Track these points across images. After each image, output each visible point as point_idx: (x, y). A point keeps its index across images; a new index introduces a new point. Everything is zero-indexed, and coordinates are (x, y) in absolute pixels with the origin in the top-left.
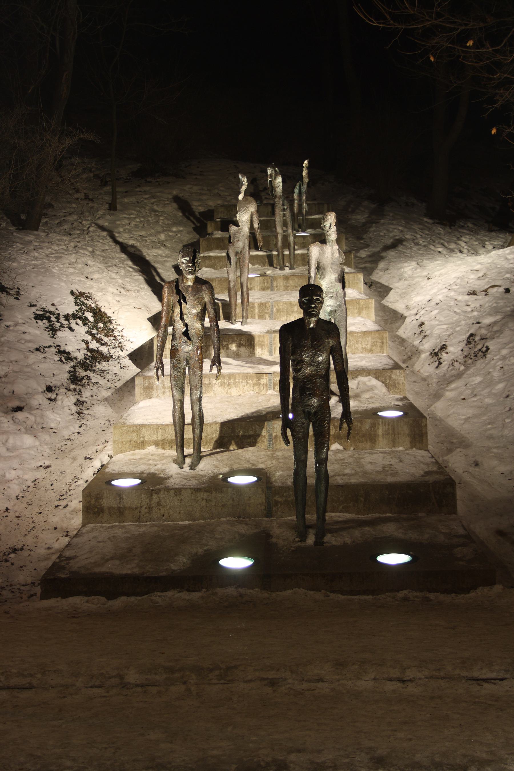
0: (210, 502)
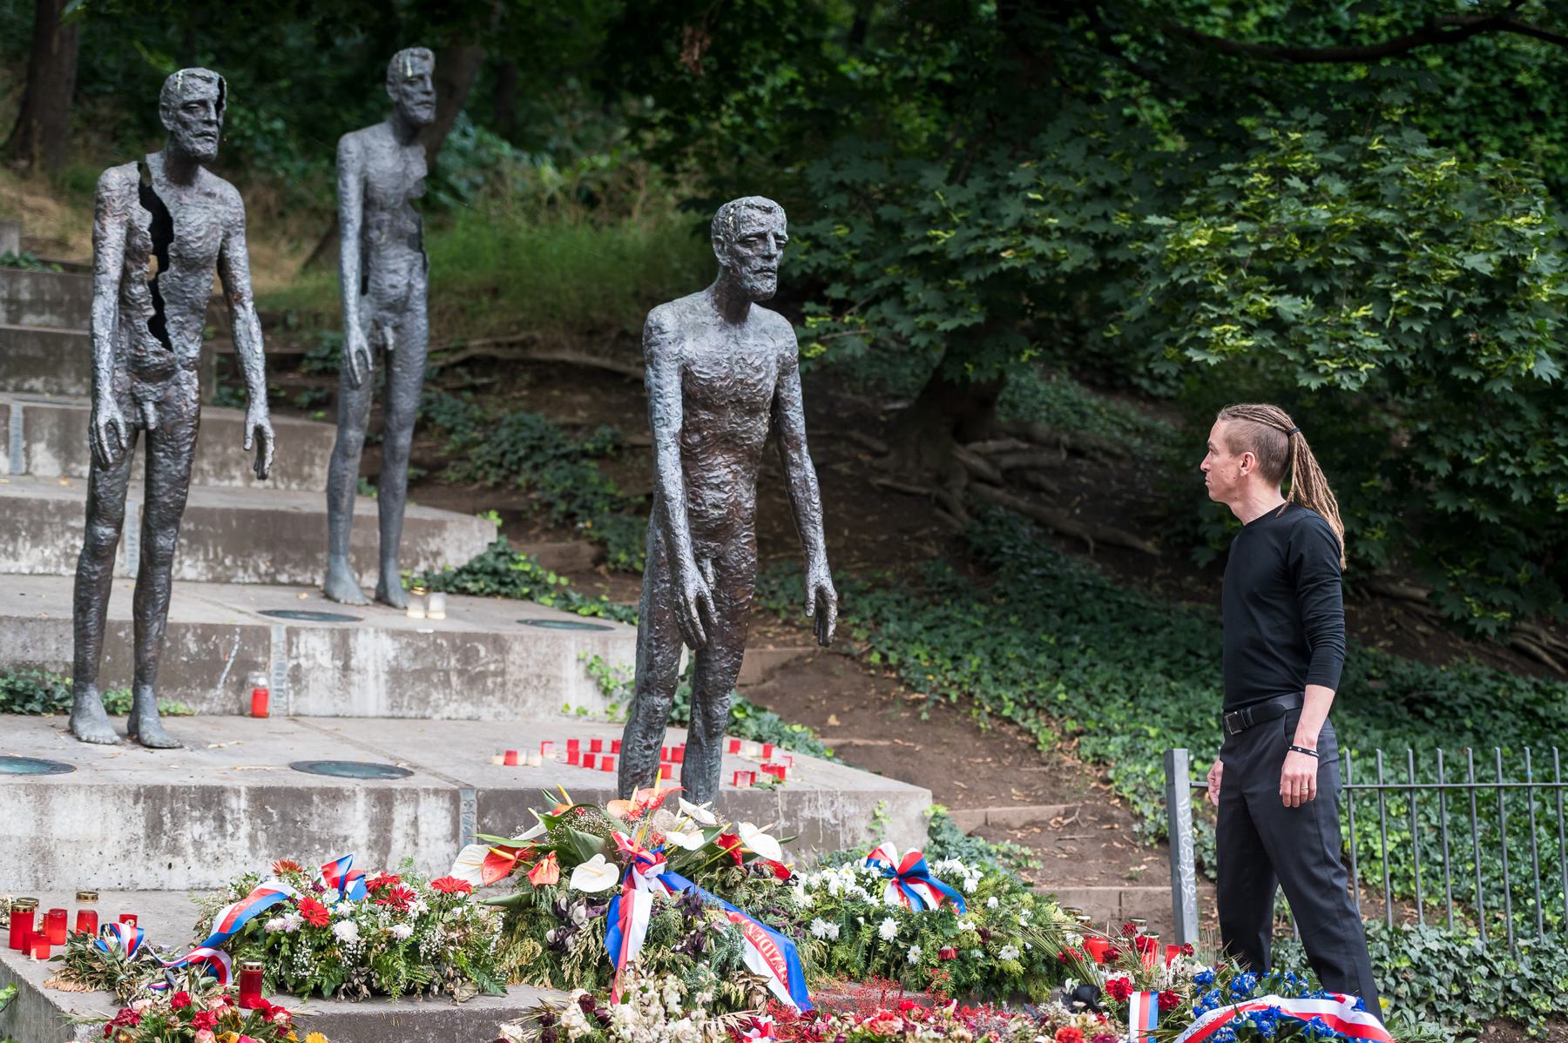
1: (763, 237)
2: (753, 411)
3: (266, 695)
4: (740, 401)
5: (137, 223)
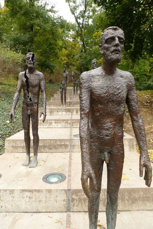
0: (32, 199)
2: (119, 103)
4: (113, 101)
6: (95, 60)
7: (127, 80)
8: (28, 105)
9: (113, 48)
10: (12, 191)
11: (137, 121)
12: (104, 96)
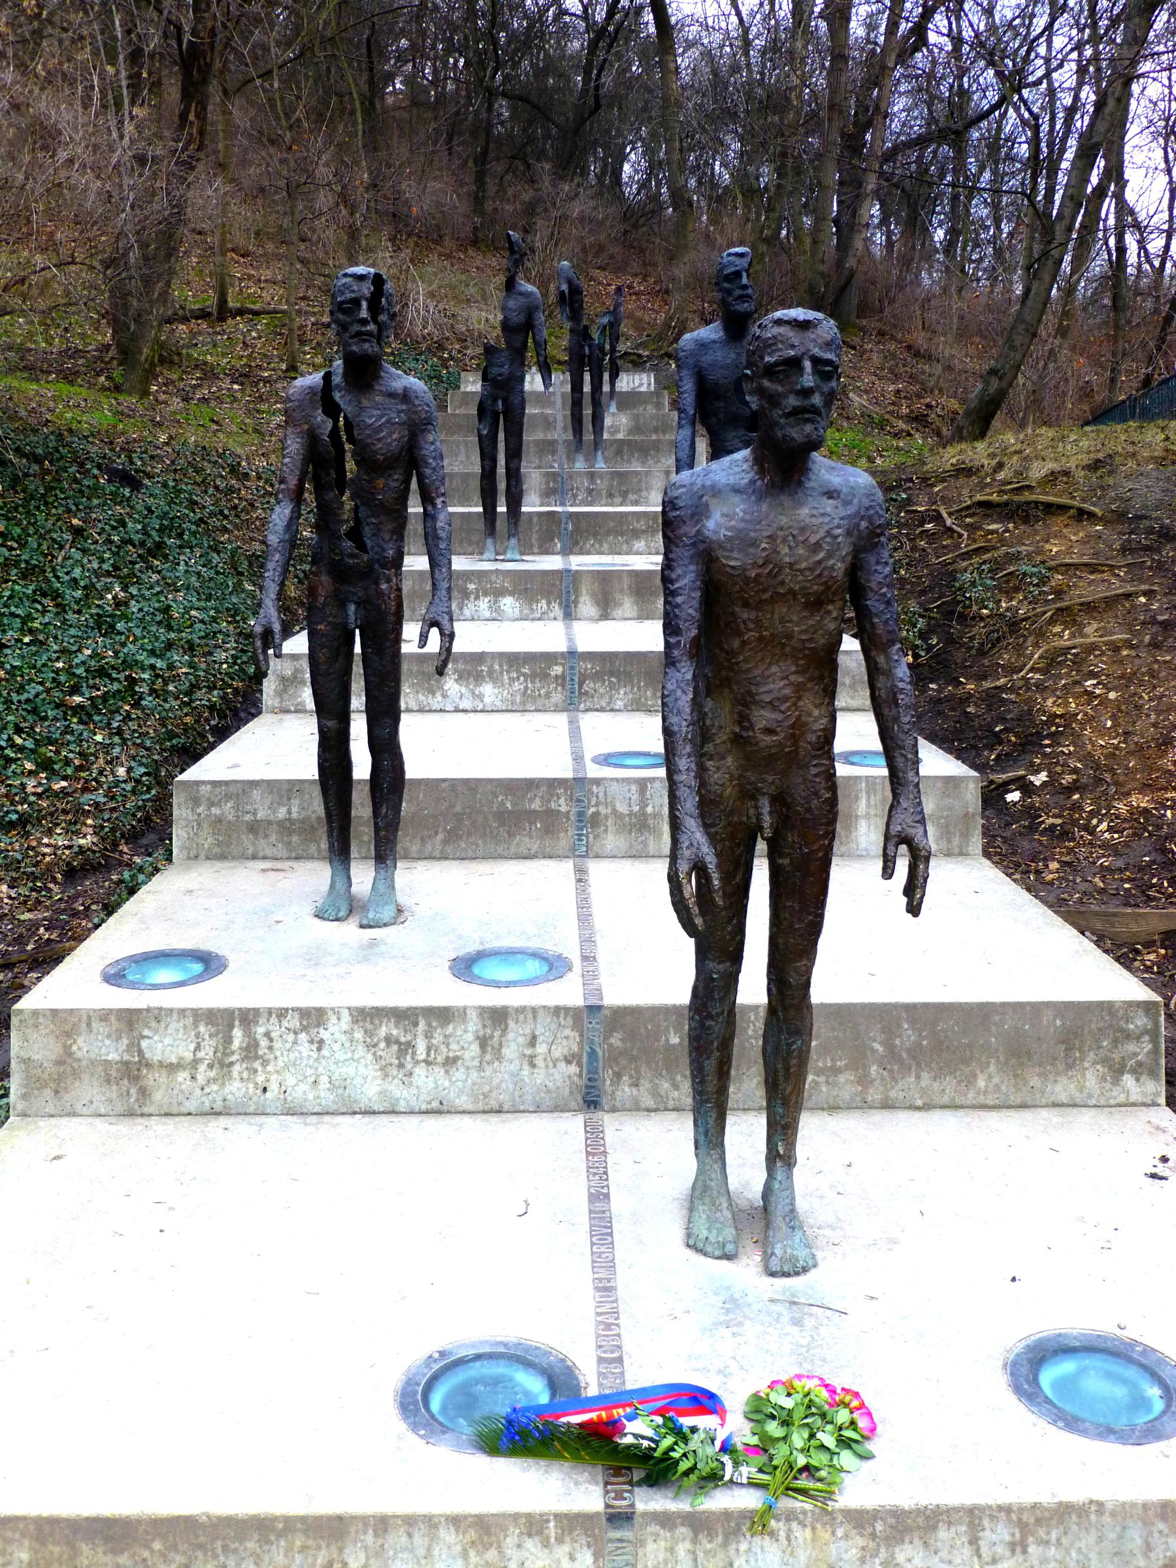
1: (794, 364)
3: (225, 967)
5: (318, 431)
6: (742, 255)
7: (850, 510)
8: (341, 573)
9: (792, 401)
10: (313, 1018)
11: (889, 673)
12: (758, 575)
